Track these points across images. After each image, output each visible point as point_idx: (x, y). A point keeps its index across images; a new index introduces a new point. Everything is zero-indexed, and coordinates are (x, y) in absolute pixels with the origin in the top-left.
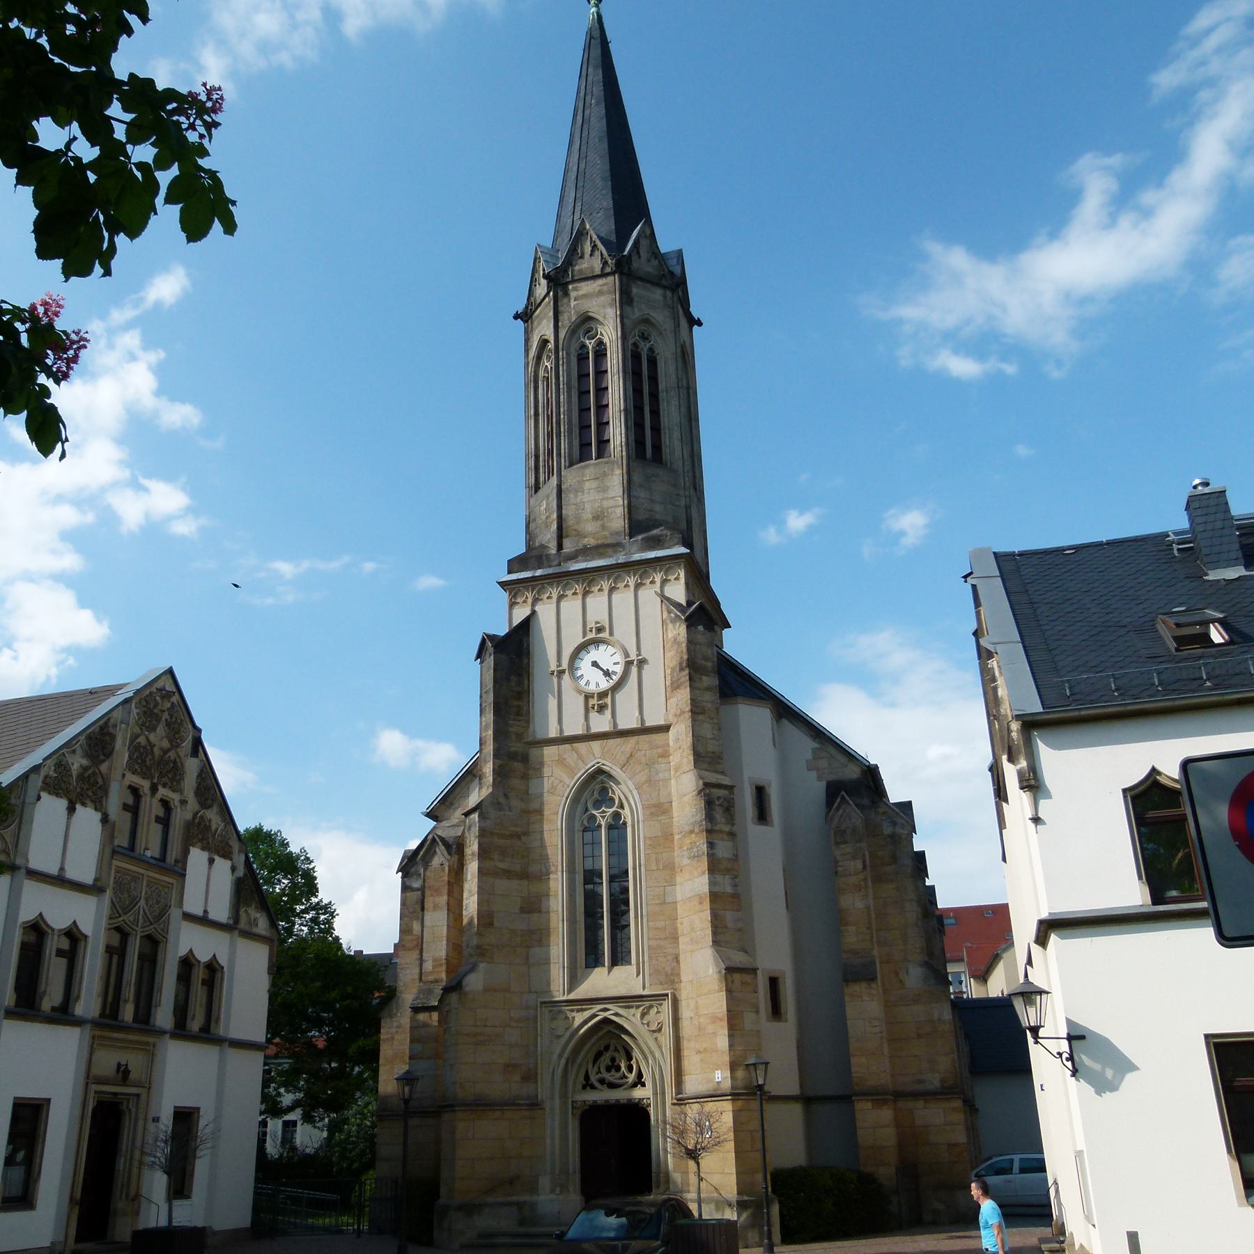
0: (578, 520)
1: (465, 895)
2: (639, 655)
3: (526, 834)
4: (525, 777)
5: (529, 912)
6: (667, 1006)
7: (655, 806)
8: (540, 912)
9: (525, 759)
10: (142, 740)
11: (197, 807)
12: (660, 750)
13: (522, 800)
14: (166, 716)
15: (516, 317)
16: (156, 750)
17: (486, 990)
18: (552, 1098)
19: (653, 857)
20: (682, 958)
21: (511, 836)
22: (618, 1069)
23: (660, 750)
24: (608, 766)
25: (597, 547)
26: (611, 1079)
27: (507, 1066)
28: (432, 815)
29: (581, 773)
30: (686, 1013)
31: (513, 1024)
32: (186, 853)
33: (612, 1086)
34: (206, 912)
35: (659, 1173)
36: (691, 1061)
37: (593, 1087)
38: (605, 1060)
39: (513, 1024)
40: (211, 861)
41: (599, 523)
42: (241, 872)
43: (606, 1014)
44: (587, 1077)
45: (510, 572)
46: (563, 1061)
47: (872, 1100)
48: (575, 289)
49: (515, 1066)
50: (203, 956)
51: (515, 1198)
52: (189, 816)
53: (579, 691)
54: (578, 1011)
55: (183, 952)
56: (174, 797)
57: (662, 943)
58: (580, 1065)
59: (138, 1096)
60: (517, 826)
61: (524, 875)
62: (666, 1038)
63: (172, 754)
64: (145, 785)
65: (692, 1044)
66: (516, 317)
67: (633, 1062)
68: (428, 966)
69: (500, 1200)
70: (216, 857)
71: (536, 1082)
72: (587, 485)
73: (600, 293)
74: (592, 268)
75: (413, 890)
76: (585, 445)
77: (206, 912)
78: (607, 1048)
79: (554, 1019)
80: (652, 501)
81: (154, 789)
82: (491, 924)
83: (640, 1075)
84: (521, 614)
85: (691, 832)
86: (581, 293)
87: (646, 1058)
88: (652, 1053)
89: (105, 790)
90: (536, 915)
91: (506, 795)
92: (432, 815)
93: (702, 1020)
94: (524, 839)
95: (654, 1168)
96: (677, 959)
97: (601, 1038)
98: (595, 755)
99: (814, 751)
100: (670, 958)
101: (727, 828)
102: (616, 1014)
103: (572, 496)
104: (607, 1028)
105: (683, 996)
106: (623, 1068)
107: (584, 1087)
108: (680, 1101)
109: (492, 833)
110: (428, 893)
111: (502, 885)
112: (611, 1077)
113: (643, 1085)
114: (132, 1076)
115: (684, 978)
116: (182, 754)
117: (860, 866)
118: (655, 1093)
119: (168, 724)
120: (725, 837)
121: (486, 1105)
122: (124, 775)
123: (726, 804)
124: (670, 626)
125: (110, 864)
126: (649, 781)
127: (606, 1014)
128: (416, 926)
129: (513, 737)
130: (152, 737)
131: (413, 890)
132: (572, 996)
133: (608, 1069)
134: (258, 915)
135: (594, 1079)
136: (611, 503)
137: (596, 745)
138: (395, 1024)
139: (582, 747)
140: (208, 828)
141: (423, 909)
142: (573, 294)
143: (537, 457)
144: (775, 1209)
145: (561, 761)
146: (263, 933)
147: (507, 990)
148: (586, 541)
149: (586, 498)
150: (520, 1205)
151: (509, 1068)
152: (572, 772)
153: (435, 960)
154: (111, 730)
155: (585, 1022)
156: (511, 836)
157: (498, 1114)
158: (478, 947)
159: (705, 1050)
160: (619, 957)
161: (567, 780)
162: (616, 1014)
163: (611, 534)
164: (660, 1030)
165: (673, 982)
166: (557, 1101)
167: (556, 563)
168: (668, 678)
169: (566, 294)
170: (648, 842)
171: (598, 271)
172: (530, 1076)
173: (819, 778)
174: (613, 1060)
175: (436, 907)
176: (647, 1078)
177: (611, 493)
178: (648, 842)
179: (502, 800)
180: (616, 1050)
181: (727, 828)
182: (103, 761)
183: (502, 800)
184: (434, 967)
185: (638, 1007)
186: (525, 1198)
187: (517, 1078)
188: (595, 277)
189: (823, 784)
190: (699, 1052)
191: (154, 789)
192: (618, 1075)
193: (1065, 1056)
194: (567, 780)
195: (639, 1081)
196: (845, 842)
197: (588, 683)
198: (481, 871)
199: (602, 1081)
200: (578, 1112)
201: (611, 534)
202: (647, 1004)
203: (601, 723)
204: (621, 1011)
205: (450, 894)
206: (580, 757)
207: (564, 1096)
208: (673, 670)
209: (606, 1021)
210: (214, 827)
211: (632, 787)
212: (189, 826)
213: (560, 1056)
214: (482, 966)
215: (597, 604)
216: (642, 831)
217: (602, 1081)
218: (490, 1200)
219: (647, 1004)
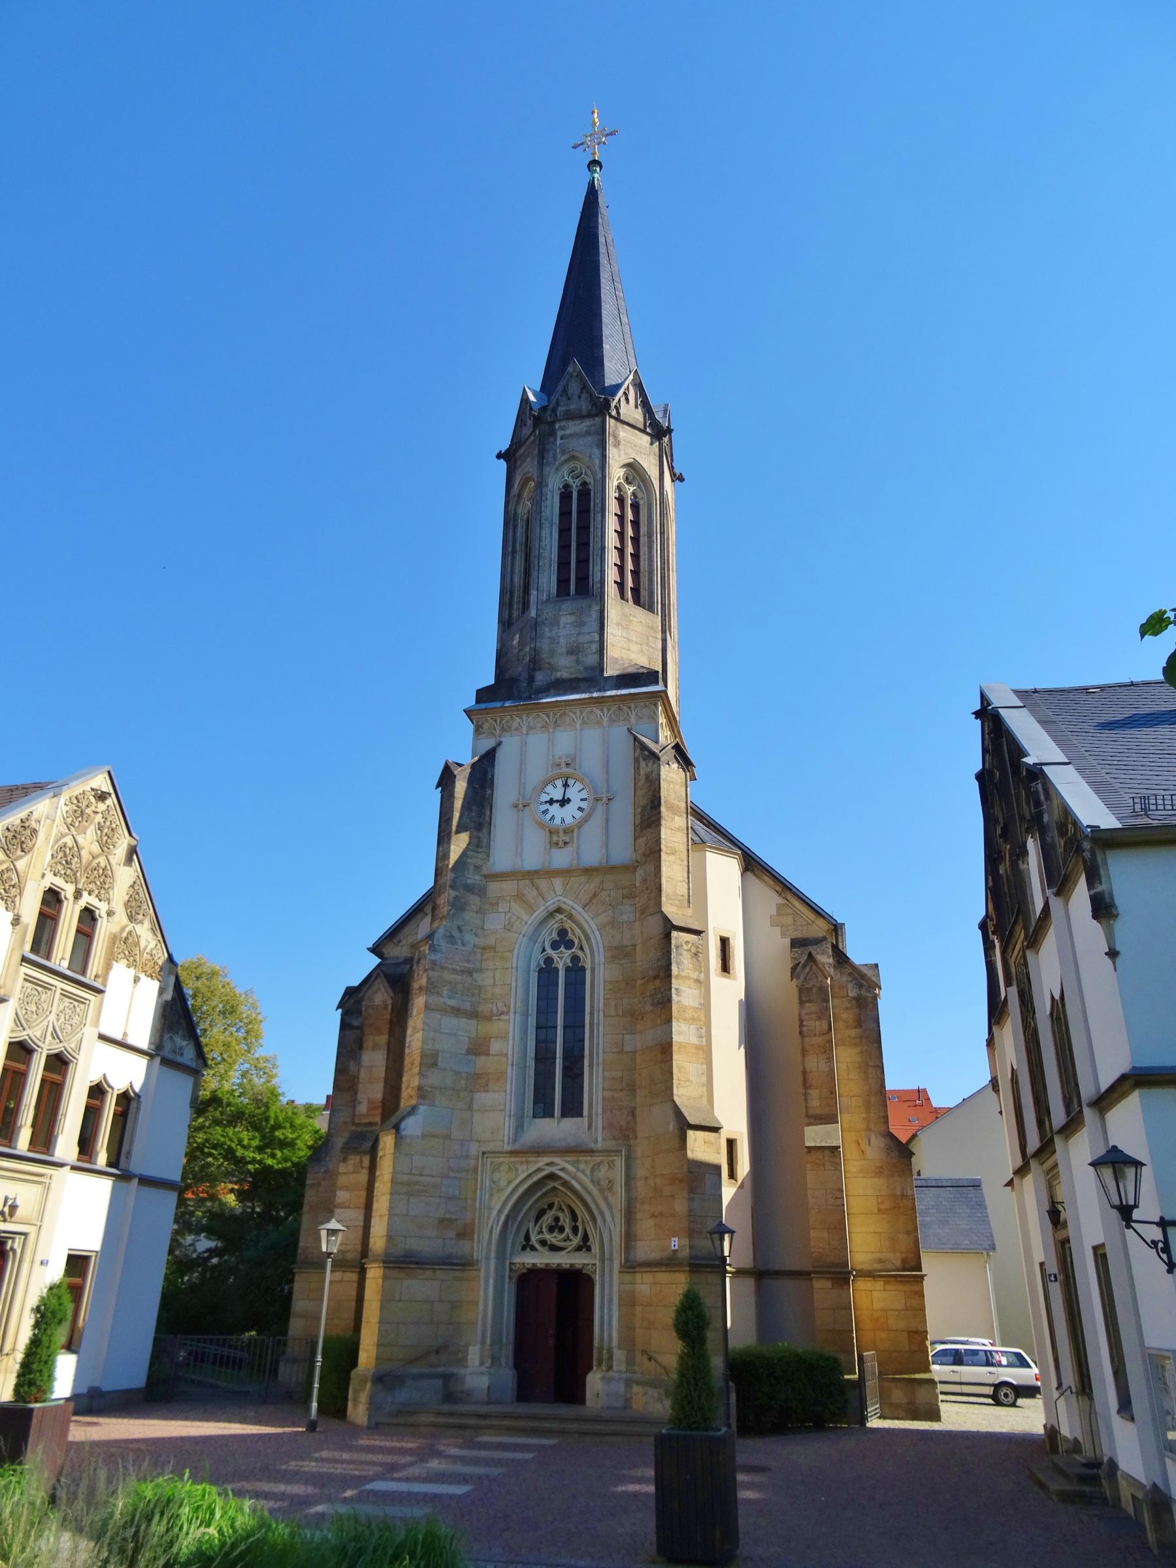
0: (552, 653)
1: (409, 1032)
2: (608, 791)
3: (480, 970)
4: (481, 911)
5: (475, 1054)
6: (620, 1162)
7: (617, 948)
8: (488, 1054)
9: (482, 892)
10: (69, 840)
11: (125, 920)
12: (625, 891)
13: (476, 935)
14: (99, 818)
15: (499, 456)
16: (84, 853)
17: (424, 1136)
18: (488, 1258)
19: (613, 1003)
20: (638, 1111)
21: (462, 972)
22: (562, 1230)
23: (625, 891)
24: (569, 903)
25: (571, 680)
26: (554, 1241)
27: (442, 1221)
28: (376, 950)
29: (540, 912)
30: (640, 1172)
31: (451, 1174)
32: (108, 967)
33: (554, 1248)
34: (125, 1034)
35: (601, 1348)
36: (645, 1225)
37: (533, 1248)
38: (547, 1219)
39: (451, 1174)
40: (136, 980)
41: (574, 657)
42: (169, 996)
43: (554, 1169)
44: (527, 1237)
45: (478, 701)
46: (503, 1217)
47: (832, 1279)
48: (563, 428)
49: (450, 1221)
50: (118, 1084)
51: (440, 1369)
52: (115, 929)
53: (541, 825)
55: (95, 1077)
56: (102, 908)
58: (521, 1223)
59: (26, 1234)
60: (468, 961)
61: (474, 1015)
62: (618, 1198)
63: (102, 861)
64: (68, 890)
65: (646, 1207)
66: (499, 456)
67: (579, 1224)
68: (362, 1108)
69: (426, 1370)
70: (142, 976)
71: (472, 1240)
72: (563, 620)
73: (587, 433)
74: (580, 410)
75: (352, 1027)
76: (563, 582)
77: (125, 1034)
78: (551, 1206)
79: (493, 1171)
80: (630, 640)
81: (78, 895)
82: (435, 1064)
83: (586, 1238)
84: (487, 744)
85: (656, 977)
86: (567, 432)
87: (594, 1219)
88: (602, 1213)
89: (20, 887)
90: (483, 1057)
91: (459, 929)
92: (376, 950)
93: (658, 1181)
94: (475, 975)
95: (596, 1343)
96: (633, 1113)
97: (544, 1195)
98: (557, 893)
99: (779, 906)
100: (625, 1111)
101: (694, 975)
102: (563, 1169)
103: (547, 629)
104: (551, 1184)
105: (639, 1151)
106: (567, 1230)
107: (524, 1248)
108: (631, 1266)
109: (443, 968)
110: (367, 1031)
111: (450, 1023)
112: (554, 1238)
113: (589, 1249)
114: (19, 1212)
115: (640, 1134)
116: (113, 860)
117: (826, 1028)
118: (602, 1260)
119: (100, 828)
120: (692, 984)
121: (417, 1263)
122: (43, 876)
123: (693, 950)
124: (643, 764)
125: (17, 971)
126: (613, 923)
128: (352, 1068)
129: (472, 868)
130: (80, 839)
131: (352, 1027)
132: (517, 1147)
133: (551, 1229)
134: (184, 1043)
135: (534, 1239)
136: (587, 638)
137: (558, 883)
138: (324, 1169)
139: (543, 884)
140: (137, 944)
141: (361, 1047)
142: (560, 433)
143: (512, 593)
144: (733, 1397)
145: (520, 897)
146: (189, 1063)
147: (447, 1137)
148: (559, 675)
149: (562, 632)
150: (447, 1378)
151: (444, 1222)
152: (531, 909)
153: (370, 1102)
154: (34, 825)
155: (529, 1176)
156: (462, 972)
157: (429, 1273)
158: (420, 1088)
159: (661, 1214)
160: (572, 1108)
161: (525, 918)
163: (586, 669)
164: (610, 1188)
165: (627, 1138)
166: (493, 1262)
167: (526, 695)
168: (638, 817)
169: (553, 433)
171: (585, 412)
172: (465, 1233)
173: (783, 935)
174: (557, 1219)
175: (375, 1047)
176: (594, 1243)
177: (587, 629)
179: (456, 934)
180: (560, 1209)
181: (694, 975)
182: (21, 857)
183: (456, 934)
184: (369, 1109)
186: (455, 1370)
187: (452, 1234)
188: (582, 417)
189: (787, 941)
190: (653, 1216)
191: (78, 895)
192: (562, 1236)
193: (1160, 1245)
194: (525, 918)
195: (584, 1246)
196: (810, 1001)
197: (553, 818)
198: (427, 1007)
199: (543, 1243)
200: (515, 1276)
201: (586, 669)
202: (598, 1159)
203: (561, 858)
204: (569, 1167)
205: (391, 1033)
206: (540, 894)
207: (501, 1256)
208: (644, 808)
209: (552, 1177)
210: (143, 944)
211: (594, 928)
212: (114, 939)
213: (500, 1211)
214: (422, 1108)
215: (564, 741)
217: (543, 1243)
218: (415, 1370)
219: (598, 1159)
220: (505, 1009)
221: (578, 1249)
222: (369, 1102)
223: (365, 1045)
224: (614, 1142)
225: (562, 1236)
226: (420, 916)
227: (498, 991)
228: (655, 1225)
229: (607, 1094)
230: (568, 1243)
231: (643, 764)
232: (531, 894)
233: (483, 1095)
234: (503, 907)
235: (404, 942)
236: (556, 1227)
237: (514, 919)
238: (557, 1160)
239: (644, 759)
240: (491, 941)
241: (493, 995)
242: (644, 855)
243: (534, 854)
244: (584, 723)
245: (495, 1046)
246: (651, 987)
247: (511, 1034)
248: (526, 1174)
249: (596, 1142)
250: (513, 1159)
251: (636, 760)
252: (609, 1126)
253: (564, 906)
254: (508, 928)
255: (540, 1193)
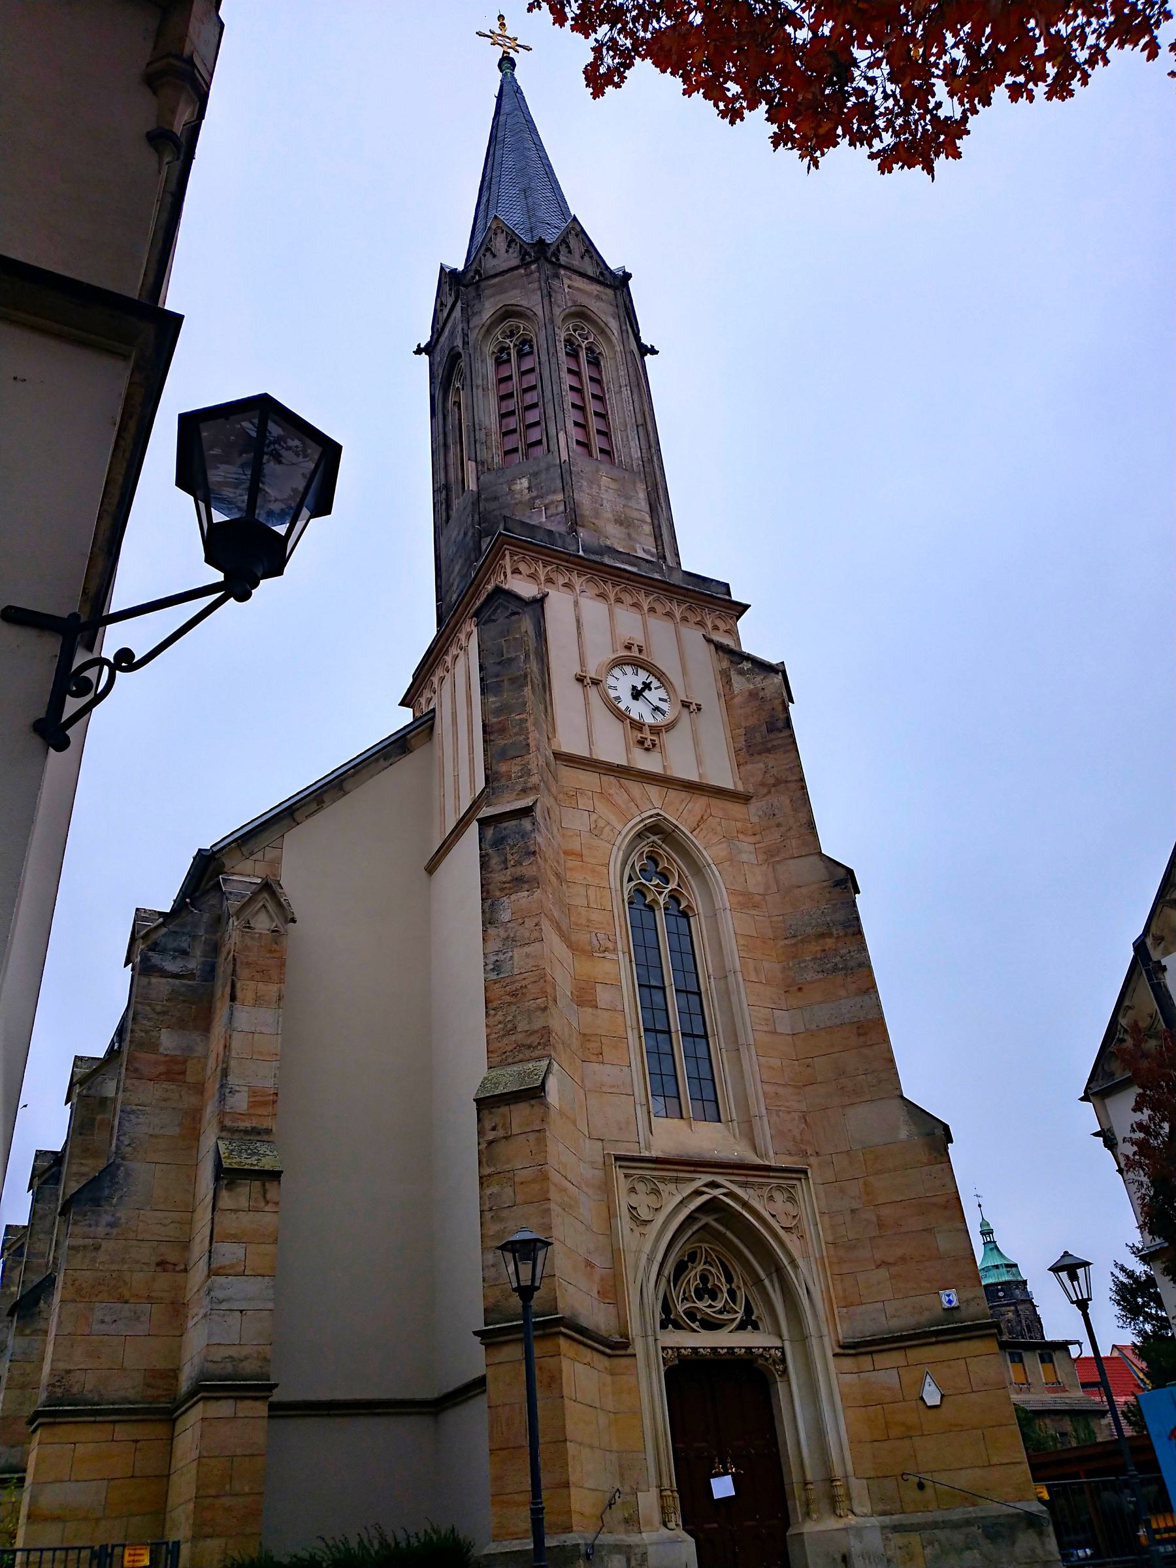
0: (597, 515)
12: (739, 824)
33: (710, 1325)
37: (678, 1326)
38: (693, 1276)
54: (677, 1180)
57: (781, 1090)
85: (822, 935)
95: (795, 1477)
100: (796, 1115)
102: (728, 1194)
107: (663, 1326)
124: (737, 680)
127: (717, 1192)
148: (608, 543)
159: (903, 1259)
162: (728, 1194)
170: (742, 942)
178: (742, 942)
184: (253, 1105)
185: (761, 1186)
208: (749, 732)
216: (730, 924)
220: (610, 945)
221: (742, 1327)
222: (253, 1092)
223: (239, 994)
224: (789, 1159)
225: (719, 1305)
226: (287, 822)
227: (595, 916)
228: (892, 1277)
229: (767, 1088)
230: (725, 1316)
231: (737, 680)
232: (620, 798)
233: (596, 1067)
234: (584, 803)
235: (259, 856)
236: (706, 1291)
237: (601, 823)
238: (719, 1179)
239: (741, 673)
240: (575, 845)
241: (588, 920)
242: (763, 784)
243: (612, 746)
244: (652, 610)
245: (604, 996)
246: (815, 948)
247: (623, 982)
248: (679, 1198)
249: (767, 1156)
250: (656, 1173)
251: (725, 676)
252: (779, 1134)
253: (664, 825)
254: (595, 832)
255: (690, 1232)
